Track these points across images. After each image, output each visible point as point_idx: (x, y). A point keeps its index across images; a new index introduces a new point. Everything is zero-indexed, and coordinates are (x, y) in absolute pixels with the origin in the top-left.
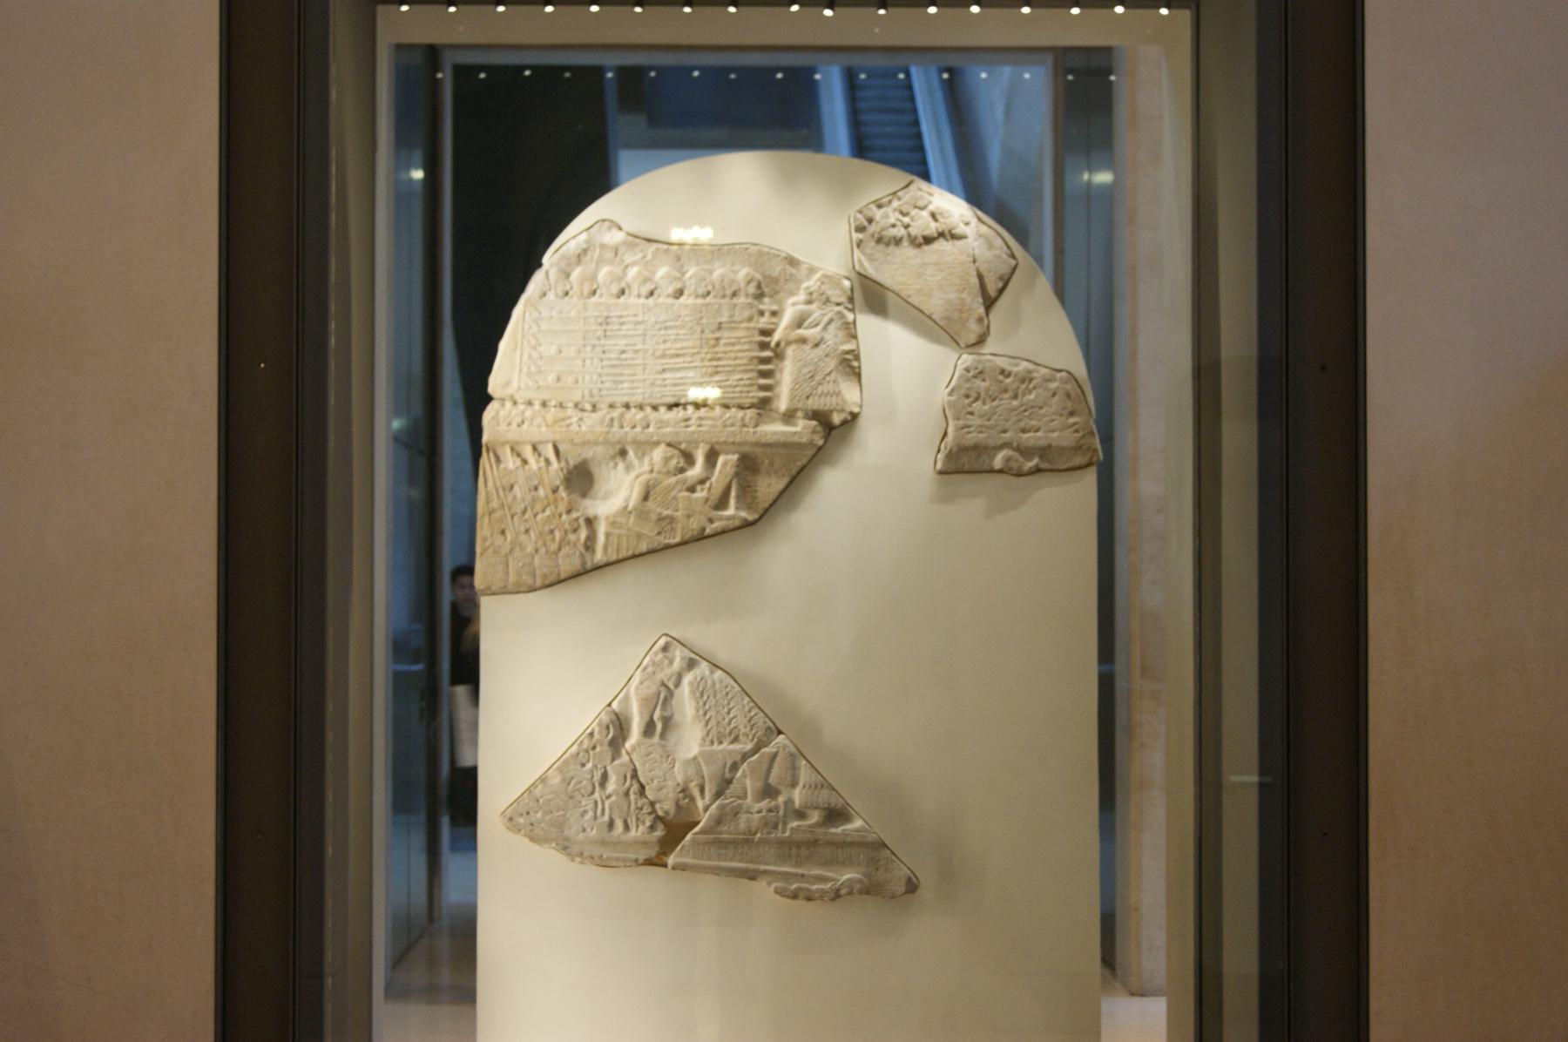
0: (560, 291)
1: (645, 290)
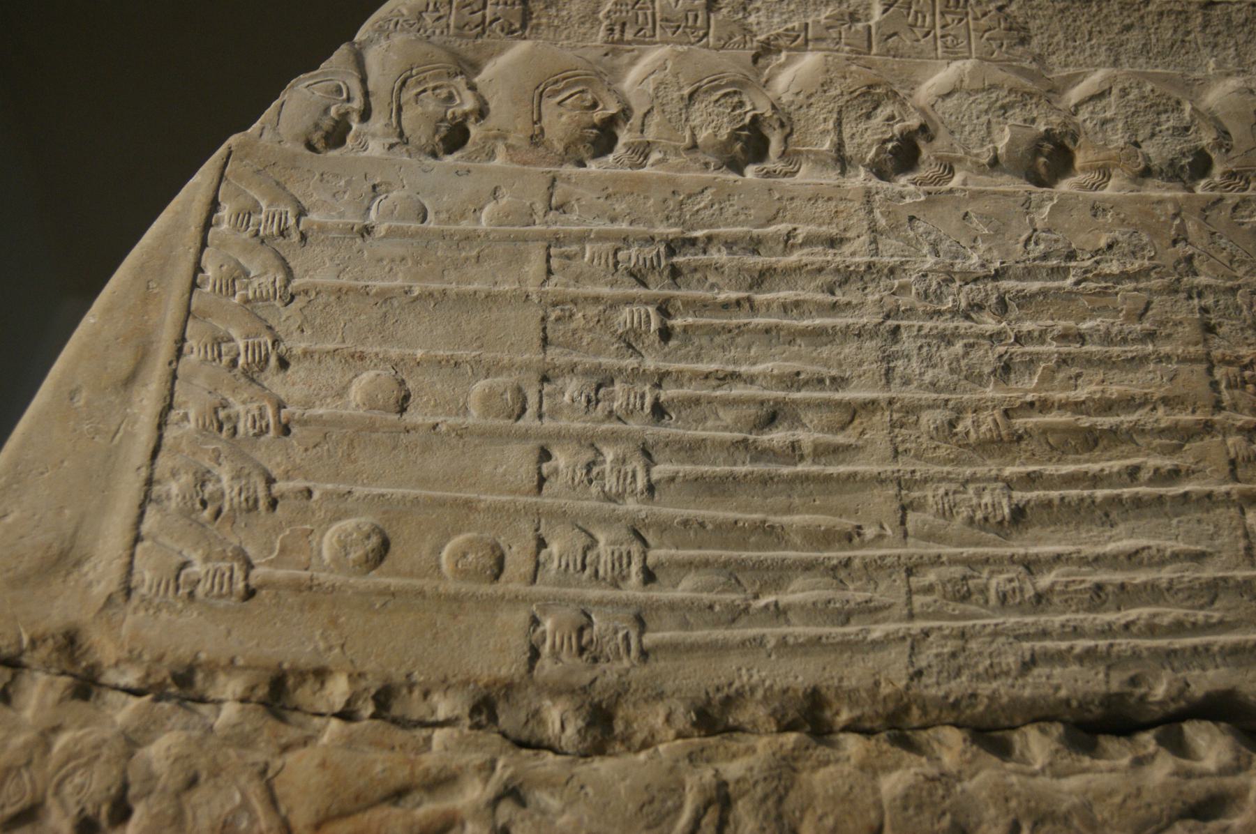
0: (420, 116)
1: (867, 137)
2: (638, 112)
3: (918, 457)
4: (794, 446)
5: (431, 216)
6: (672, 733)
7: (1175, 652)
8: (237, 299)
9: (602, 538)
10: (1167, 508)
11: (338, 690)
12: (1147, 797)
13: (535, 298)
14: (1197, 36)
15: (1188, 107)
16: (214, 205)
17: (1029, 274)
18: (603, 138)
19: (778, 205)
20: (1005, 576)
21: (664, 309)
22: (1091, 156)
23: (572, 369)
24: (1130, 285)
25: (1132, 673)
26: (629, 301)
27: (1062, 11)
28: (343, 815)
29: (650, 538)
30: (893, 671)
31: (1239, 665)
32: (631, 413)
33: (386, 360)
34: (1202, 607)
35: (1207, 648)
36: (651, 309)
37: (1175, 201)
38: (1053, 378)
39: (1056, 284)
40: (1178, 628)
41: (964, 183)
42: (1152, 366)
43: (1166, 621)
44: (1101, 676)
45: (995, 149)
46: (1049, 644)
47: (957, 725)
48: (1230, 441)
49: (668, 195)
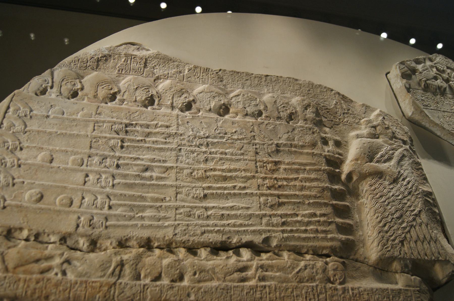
0: (66, 88)
1: (180, 101)
2: (122, 92)
3: (182, 181)
4: (151, 177)
5: (65, 114)
6: (111, 247)
7: (239, 231)
8: (11, 132)
9: (99, 197)
10: (242, 196)
11: (25, 233)
12: (228, 266)
13: (89, 136)
14: (263, 83)
15: (258, 100)
16: (8, 108)
17: (215, 137)
18: (113, 97)
19: (155, 117)
20: (200, 211)
21: (122, 141)
22: (234, 110)
23: (97, 155)
24: (239, 142)
25: (228, 236)
26: (114, 138)
27: (232, 75)
28: (22, 265)
29: (112, 198)
30: (169, 233)
31: (255, 235)
32: (110, 166)
33: (48, 149)
34: (247, 221)
35: (247, 230)
36: (119, 141)
37: (252, 122)
38: (218, 163)
39: (221, 140)
40: (241, 225)
41: (202, 114)
42: (242, 162)
43: (238, 223)
44: (221, 236)
45: (211, 107)
46: (209, 228)
47: (184, 247)
48: (259, 180)
49: (127, 112)
